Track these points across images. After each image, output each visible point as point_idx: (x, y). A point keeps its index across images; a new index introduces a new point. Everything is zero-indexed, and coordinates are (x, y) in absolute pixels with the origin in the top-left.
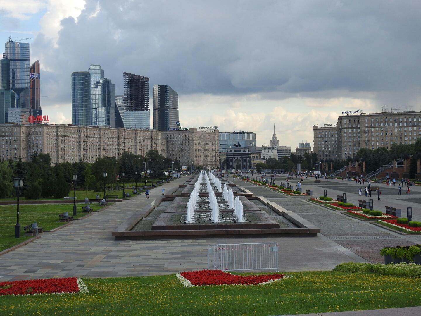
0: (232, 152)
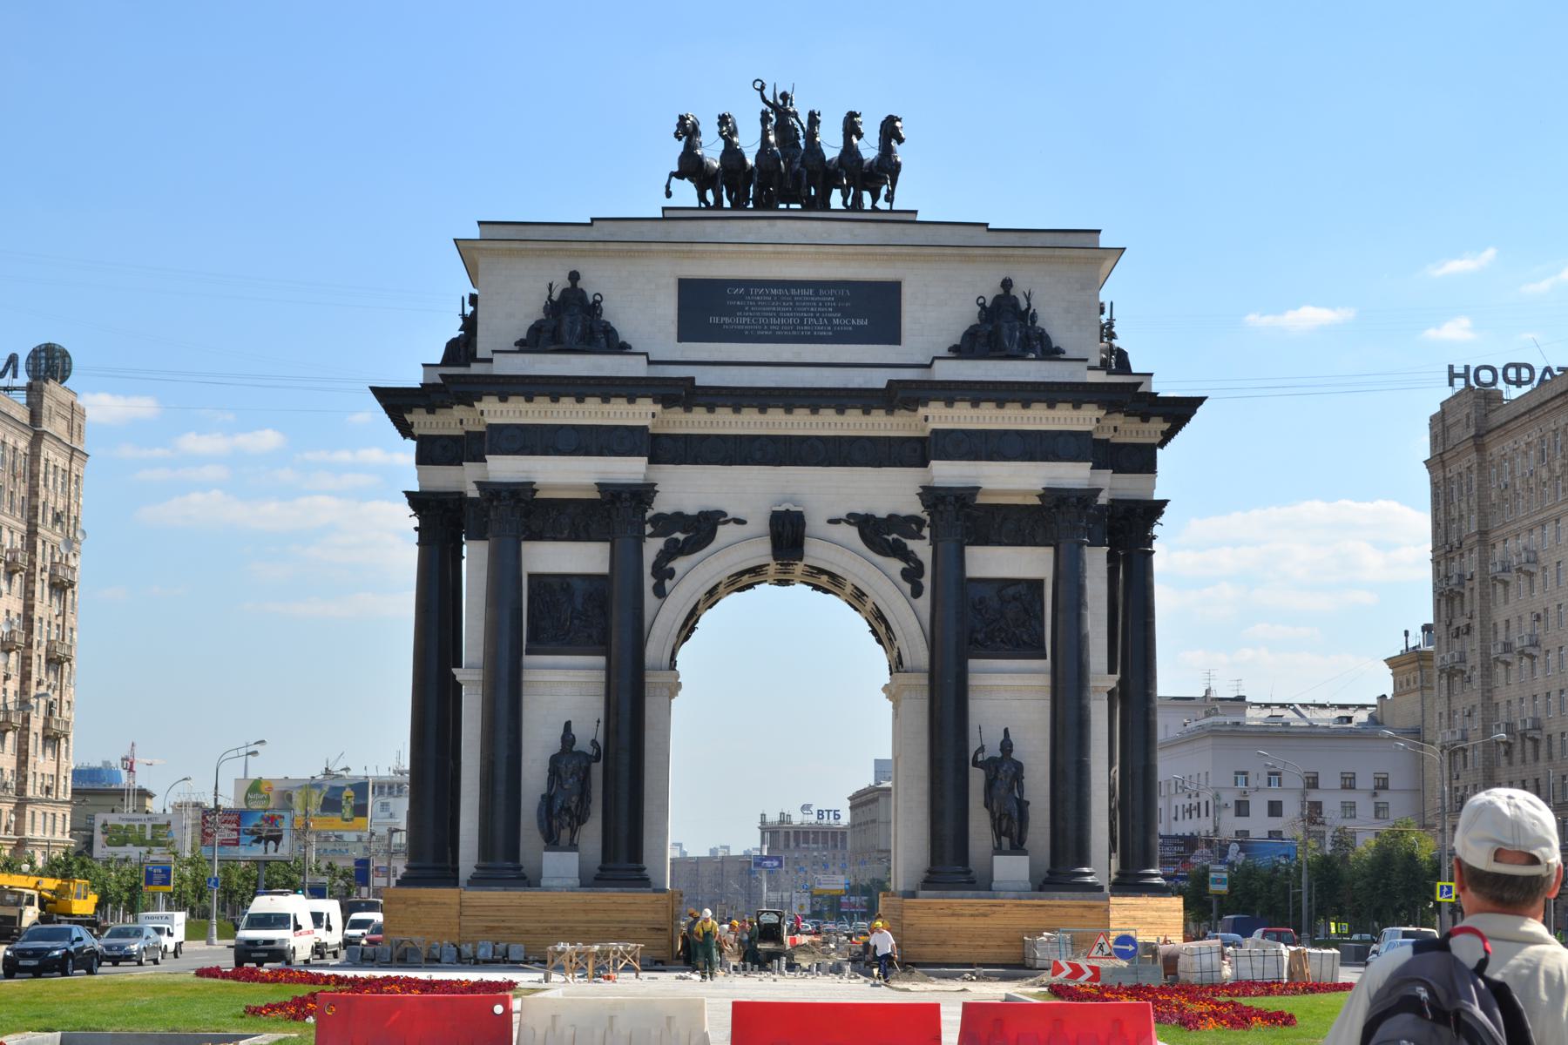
0: (608, 341)
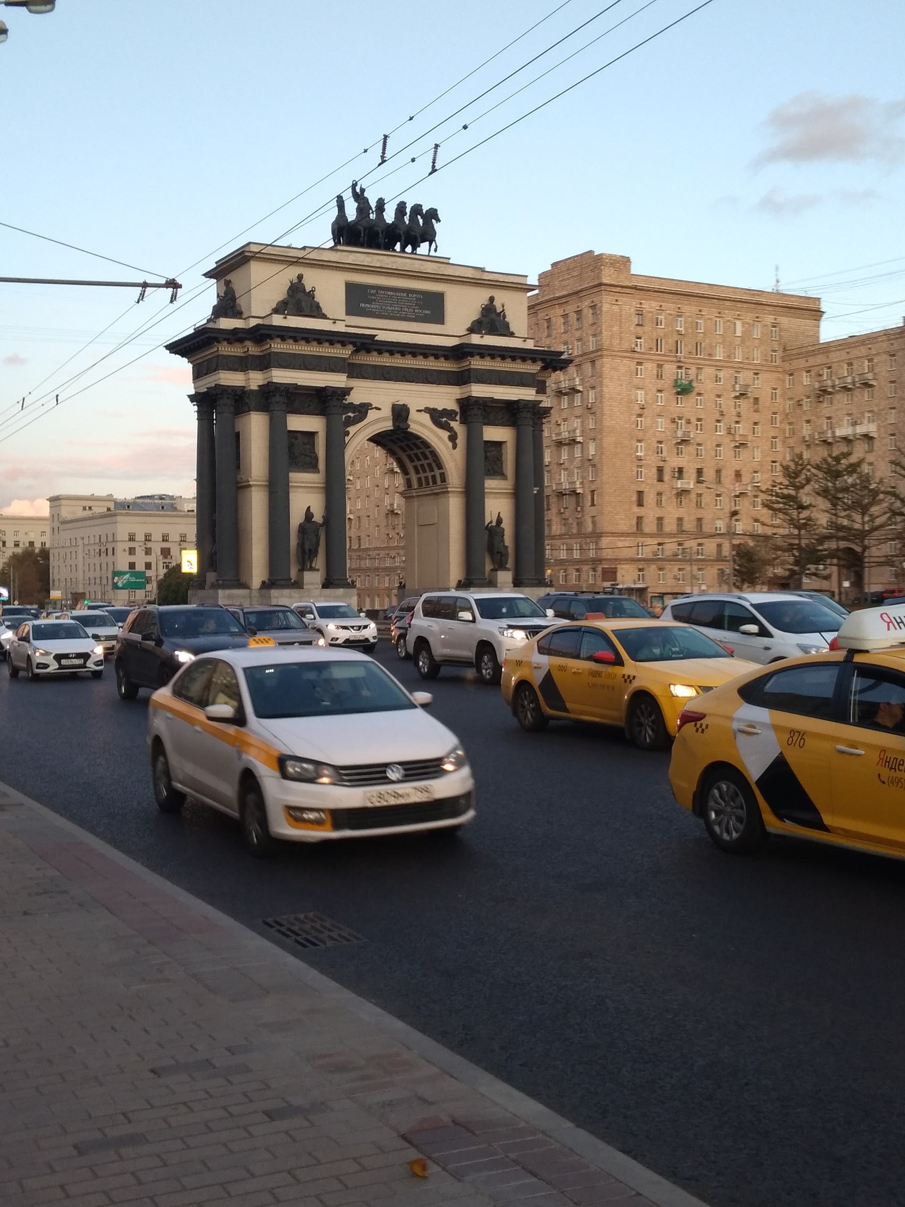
0: (316, 312)
